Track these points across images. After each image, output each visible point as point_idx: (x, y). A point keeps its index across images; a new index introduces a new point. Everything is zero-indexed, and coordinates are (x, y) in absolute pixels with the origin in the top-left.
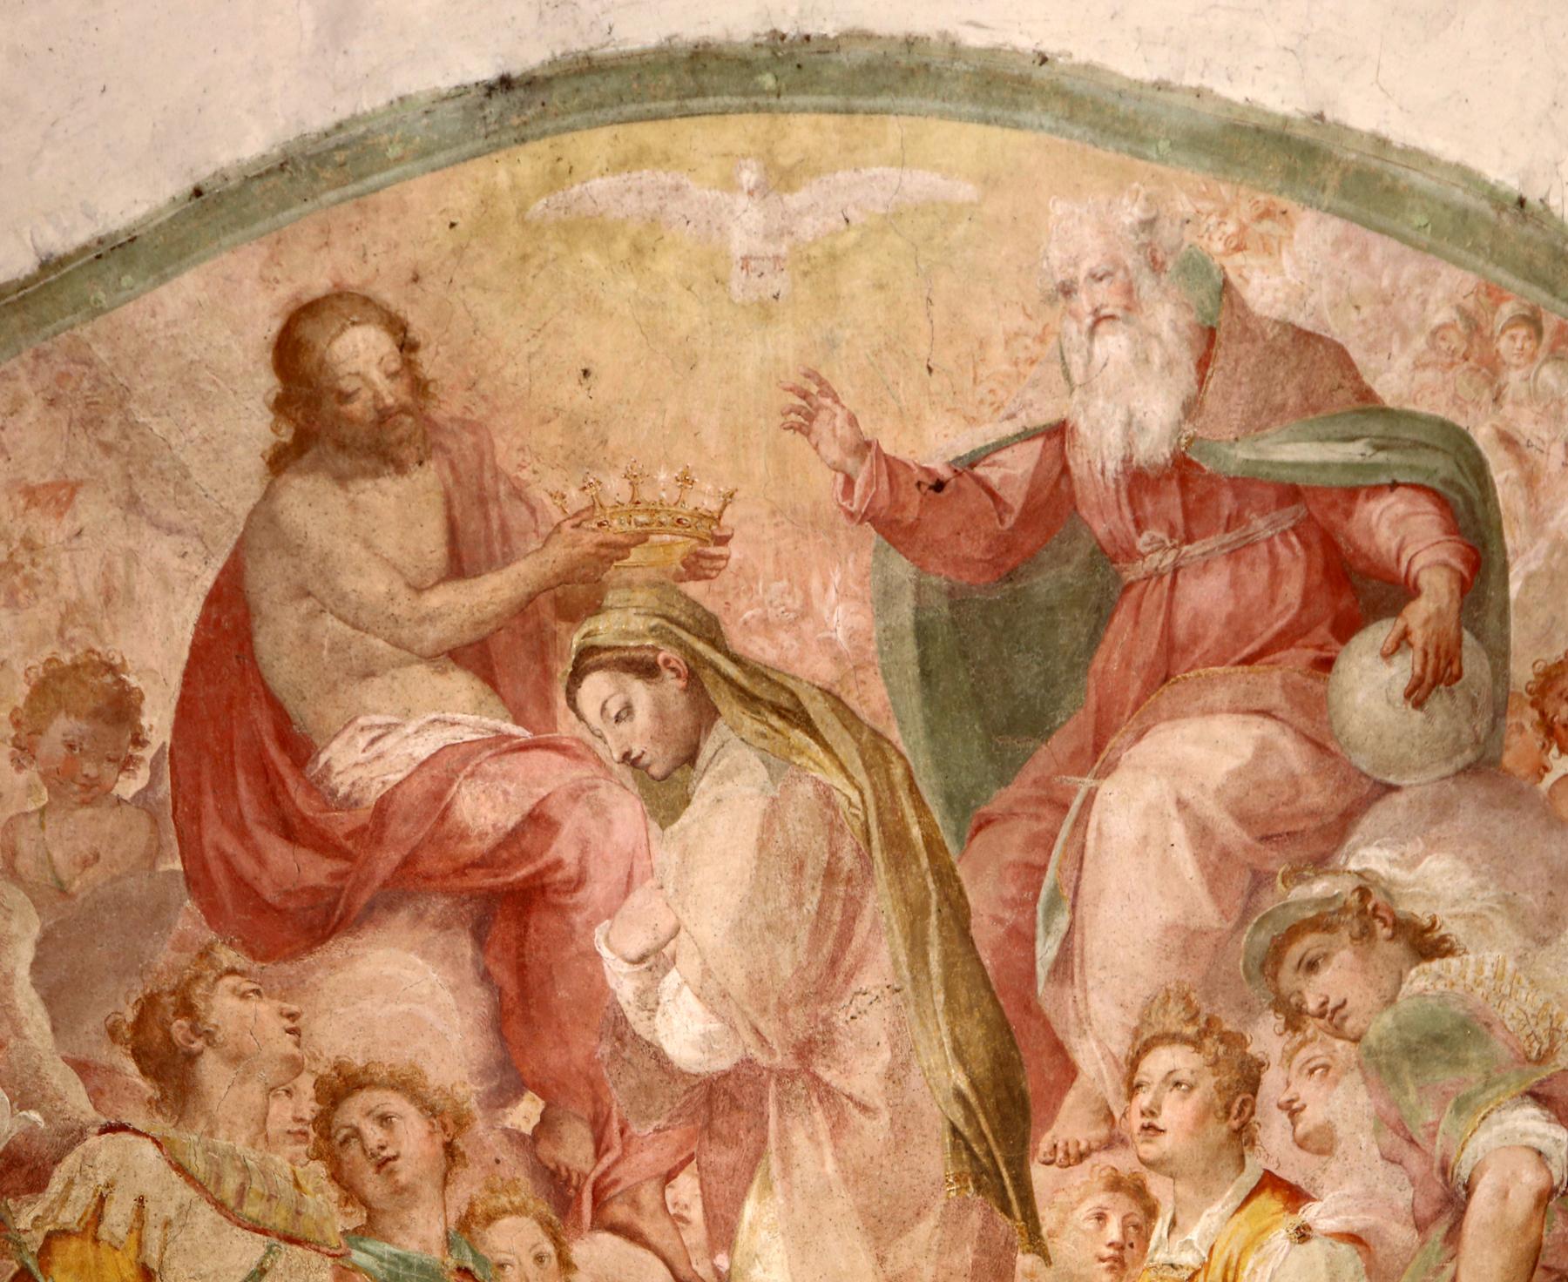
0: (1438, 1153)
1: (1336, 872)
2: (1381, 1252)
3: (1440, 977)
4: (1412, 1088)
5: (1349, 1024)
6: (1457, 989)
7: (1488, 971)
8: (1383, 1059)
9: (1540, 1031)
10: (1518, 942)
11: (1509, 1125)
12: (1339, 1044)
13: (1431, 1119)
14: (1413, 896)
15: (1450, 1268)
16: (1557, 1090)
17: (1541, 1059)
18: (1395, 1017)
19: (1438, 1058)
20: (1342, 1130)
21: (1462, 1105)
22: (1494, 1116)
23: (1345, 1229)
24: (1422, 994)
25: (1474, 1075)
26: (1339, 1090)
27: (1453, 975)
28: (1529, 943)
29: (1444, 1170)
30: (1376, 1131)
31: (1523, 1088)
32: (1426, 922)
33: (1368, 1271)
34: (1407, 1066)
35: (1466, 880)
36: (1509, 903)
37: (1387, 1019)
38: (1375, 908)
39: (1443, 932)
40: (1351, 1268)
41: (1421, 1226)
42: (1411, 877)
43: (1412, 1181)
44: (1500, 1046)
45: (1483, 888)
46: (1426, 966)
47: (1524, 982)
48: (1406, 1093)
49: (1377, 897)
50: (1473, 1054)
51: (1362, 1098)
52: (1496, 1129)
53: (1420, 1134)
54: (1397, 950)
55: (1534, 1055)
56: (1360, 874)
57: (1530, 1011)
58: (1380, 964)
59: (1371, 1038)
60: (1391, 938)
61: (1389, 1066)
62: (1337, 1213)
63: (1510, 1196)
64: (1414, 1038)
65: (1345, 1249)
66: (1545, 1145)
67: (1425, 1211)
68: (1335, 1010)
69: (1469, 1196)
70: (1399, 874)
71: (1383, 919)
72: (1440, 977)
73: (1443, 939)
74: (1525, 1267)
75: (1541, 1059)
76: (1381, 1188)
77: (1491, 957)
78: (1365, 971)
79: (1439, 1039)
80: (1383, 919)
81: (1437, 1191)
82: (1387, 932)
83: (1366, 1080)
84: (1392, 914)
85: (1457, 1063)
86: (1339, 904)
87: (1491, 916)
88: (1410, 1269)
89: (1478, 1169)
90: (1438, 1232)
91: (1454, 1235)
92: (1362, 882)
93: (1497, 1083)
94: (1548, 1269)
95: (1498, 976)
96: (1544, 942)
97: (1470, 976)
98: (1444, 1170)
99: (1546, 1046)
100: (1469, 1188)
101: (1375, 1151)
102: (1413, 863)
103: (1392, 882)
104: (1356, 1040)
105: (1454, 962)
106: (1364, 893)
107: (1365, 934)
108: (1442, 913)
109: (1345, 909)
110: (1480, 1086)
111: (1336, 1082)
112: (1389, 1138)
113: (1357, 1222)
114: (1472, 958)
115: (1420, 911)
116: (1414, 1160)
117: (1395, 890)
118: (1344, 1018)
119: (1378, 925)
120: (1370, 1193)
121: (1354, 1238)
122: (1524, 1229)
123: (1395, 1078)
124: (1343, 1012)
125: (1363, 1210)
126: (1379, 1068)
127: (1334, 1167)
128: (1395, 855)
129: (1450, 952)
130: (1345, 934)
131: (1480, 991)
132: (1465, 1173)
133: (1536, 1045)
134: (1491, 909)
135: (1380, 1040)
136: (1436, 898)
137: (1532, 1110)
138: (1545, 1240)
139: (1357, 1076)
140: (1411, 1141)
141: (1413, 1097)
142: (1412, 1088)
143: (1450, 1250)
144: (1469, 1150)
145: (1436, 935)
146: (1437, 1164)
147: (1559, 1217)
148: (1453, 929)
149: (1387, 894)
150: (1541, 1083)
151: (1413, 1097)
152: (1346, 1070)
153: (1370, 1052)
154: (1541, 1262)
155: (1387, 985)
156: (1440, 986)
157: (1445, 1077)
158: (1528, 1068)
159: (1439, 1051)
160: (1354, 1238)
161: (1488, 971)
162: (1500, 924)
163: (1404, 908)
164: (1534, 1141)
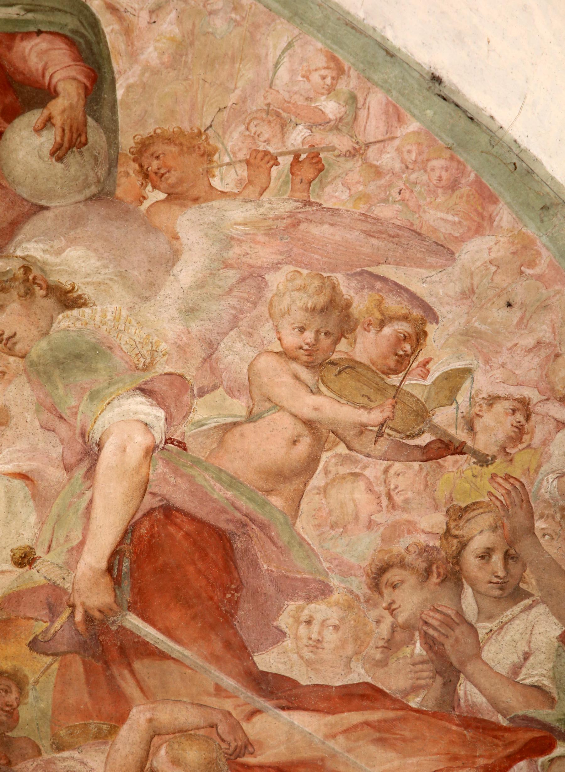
0: (79, 424)
1: (8, 257)
2: (41, 485)
3: (78, 319)
4: (60, 386)
5: (18, 347)
6: (89, 327)
7: (109, 316)
8: (41, 368)
9: (144, 351)
10: (128, 299)
11: (125, 408)
12: (11, 359)
13: (73, 404)
14: (59, 271)
15: (88, 494)
16: (157, 386)
17: (146, 368)
18: (49, 343)
19: (77, 368)
20: (14, 411)
21: (94, 396)
22: (116, 402)
23: (17, 470)
24: (67, 330)
25: (102, 378)
26: (12, 387)
27: (87, 318)
28: (137, 299)
29: (83, 435)
30: (37, 411)
31: (134, 385)
32: (69, 287)
33: (34, 496)
34: (57, 372)
35: (94, 262)
36: (122, 276)
37: (44, 344)
38: (34, 278)
39: (79, 292)
40: (22, 494)
41: (68, 469)
42: (58, 260)
43: (62, 441)
44: (118, 360)
45: (106, 267)
46: (69, 313)
47: (134, 322)
48: (57, 389)
49: (35, 272)
50: (101, 365)
51: (27, 391)
52: (117, 410)
53: (66, 414)
54: (50, 303)
55: (141, 366)
56: (24, 258)
57: (138, 340)
58: (38, 311)
59: (33, 355)
60: (46, 296)
61: (45, 373)
62: (11, 461)
63: (127, 450)
64: (61, 356)
65: (17, 483)
66: (149, 420)
67: (71, 459)
68: (8, 339)
69: (100, 450)
70: (50, 258)
71: (39, 285)
72: (78, 319)
73: (80, 297)
74: (138, 493)
75: (146, 368)
76: (41, 445)
77: (111, 308)
78: (28, 316)
79: (78, 357)
80: (39, 285)
81: (79, 447)
82: (43, 292)
83: (30, 381)
84: (46, 282)
85: (90, 370)
86: (10, 276)
87: (111, 283)
88: (62, 494)
89: (106, 434)
90: (79, 472)
91: (90, 473)
92: (25, 263)
93: (117, 382)
94: (153, 494)
95: (116, 319)
96: (146, 299)
97: (98, 319)
98: (83, 435)
99: (148, 360)
100: (100, 446)
101: (37, 423)
102: (59, 252)
103: (45, 263)
104: (23, 357)
105: (87, 311)
106: (27, 269)
107: (29, 293)
108: (78, 282)
109: (14, 278)
110: (106, 384)
111: (10, 382)
112: (46, 416)
113: (25, 466)
114: (99, 308)
115: (65, 281)
116: (63, 429)
117: (47, 268)
118: (15, 344)
119: (37, 288)
120: (34, 449)
121: (23, 476)
122: (137, 470)
123: (49, 378)
124: (13, 340)
125: (29, 459)
126: (38, 373)
127: (9, 433)
128: (47, 247)
129: (85, 304)
130: (14, 293)
131: (104, 328)
132: (97, 437)
133: (142, 360)
134: (111, 279)
135: (39, 357)
136: (74, 272)
137: (140, 399)
138: (151, 476)
139: (24, 378)
140: (61, 417)
141: (61, 391)
142: (60, 386)
143: (88, 483)
144: (99, 422)
145: (75, 295)
146: (78, 431)
147: (160, 463)
148: (87, 291)
149: (42, 270)
150: (146, 383)
151: (61, 391)
152: (17, 375)
153: (32, 364)
154: (149, 490)
155: (43, 324)
156: (78, 325)
157: (83, 379)
158: (137, 373)
159: (78, 363)
160: (23, 476)
161: (109, 316)
162: (117, 288)
163: (53, 279)
164: (142, 417)
